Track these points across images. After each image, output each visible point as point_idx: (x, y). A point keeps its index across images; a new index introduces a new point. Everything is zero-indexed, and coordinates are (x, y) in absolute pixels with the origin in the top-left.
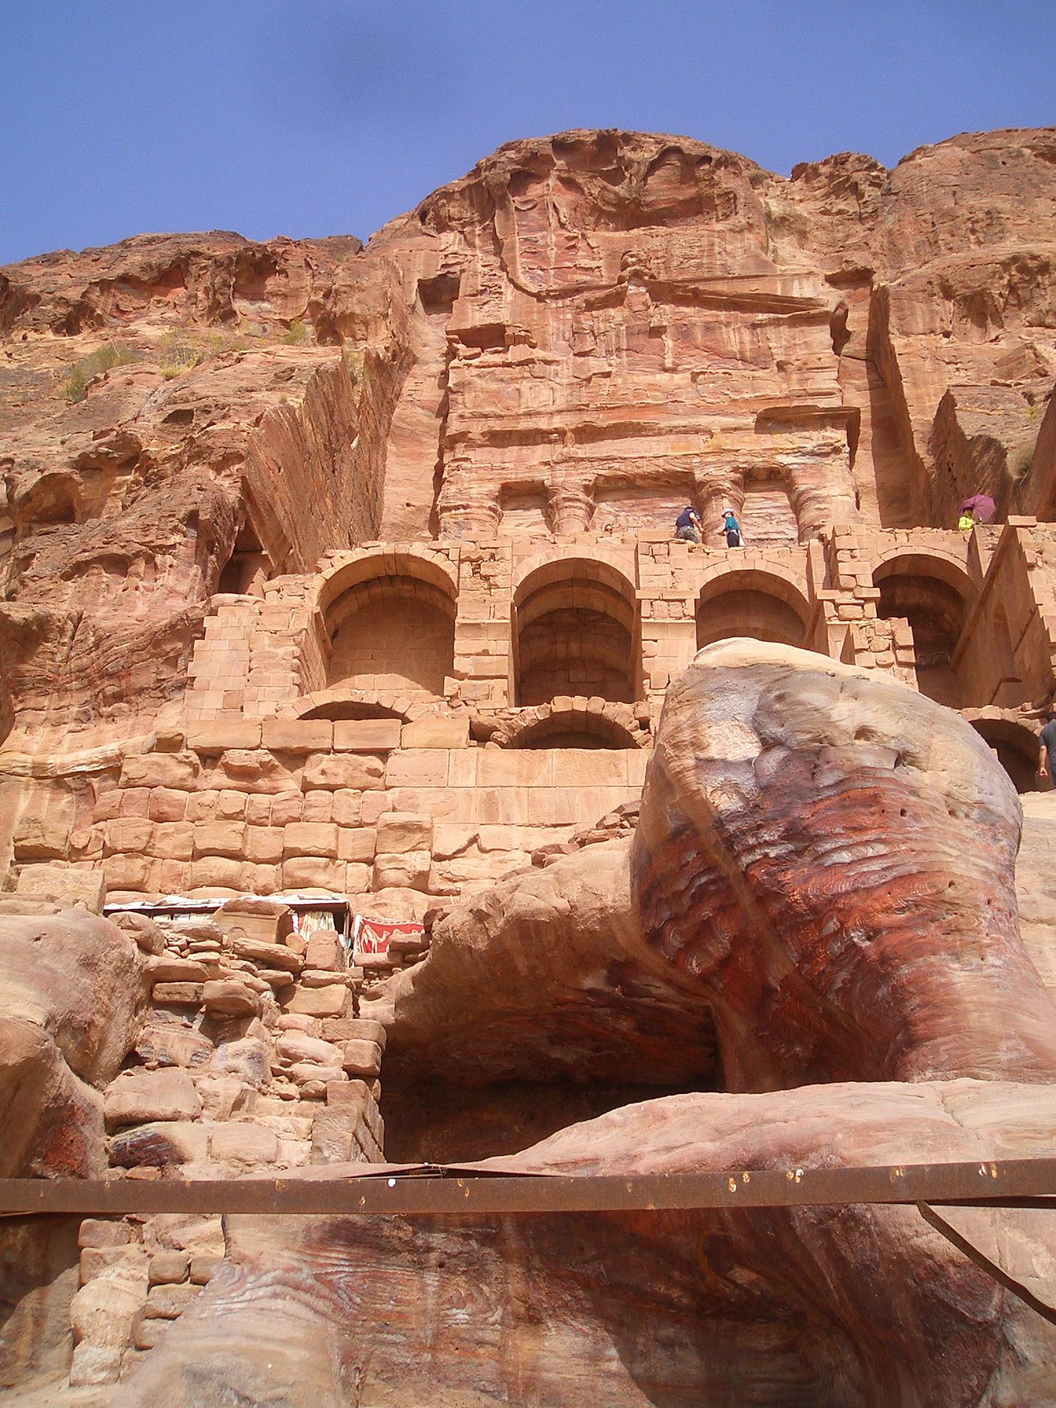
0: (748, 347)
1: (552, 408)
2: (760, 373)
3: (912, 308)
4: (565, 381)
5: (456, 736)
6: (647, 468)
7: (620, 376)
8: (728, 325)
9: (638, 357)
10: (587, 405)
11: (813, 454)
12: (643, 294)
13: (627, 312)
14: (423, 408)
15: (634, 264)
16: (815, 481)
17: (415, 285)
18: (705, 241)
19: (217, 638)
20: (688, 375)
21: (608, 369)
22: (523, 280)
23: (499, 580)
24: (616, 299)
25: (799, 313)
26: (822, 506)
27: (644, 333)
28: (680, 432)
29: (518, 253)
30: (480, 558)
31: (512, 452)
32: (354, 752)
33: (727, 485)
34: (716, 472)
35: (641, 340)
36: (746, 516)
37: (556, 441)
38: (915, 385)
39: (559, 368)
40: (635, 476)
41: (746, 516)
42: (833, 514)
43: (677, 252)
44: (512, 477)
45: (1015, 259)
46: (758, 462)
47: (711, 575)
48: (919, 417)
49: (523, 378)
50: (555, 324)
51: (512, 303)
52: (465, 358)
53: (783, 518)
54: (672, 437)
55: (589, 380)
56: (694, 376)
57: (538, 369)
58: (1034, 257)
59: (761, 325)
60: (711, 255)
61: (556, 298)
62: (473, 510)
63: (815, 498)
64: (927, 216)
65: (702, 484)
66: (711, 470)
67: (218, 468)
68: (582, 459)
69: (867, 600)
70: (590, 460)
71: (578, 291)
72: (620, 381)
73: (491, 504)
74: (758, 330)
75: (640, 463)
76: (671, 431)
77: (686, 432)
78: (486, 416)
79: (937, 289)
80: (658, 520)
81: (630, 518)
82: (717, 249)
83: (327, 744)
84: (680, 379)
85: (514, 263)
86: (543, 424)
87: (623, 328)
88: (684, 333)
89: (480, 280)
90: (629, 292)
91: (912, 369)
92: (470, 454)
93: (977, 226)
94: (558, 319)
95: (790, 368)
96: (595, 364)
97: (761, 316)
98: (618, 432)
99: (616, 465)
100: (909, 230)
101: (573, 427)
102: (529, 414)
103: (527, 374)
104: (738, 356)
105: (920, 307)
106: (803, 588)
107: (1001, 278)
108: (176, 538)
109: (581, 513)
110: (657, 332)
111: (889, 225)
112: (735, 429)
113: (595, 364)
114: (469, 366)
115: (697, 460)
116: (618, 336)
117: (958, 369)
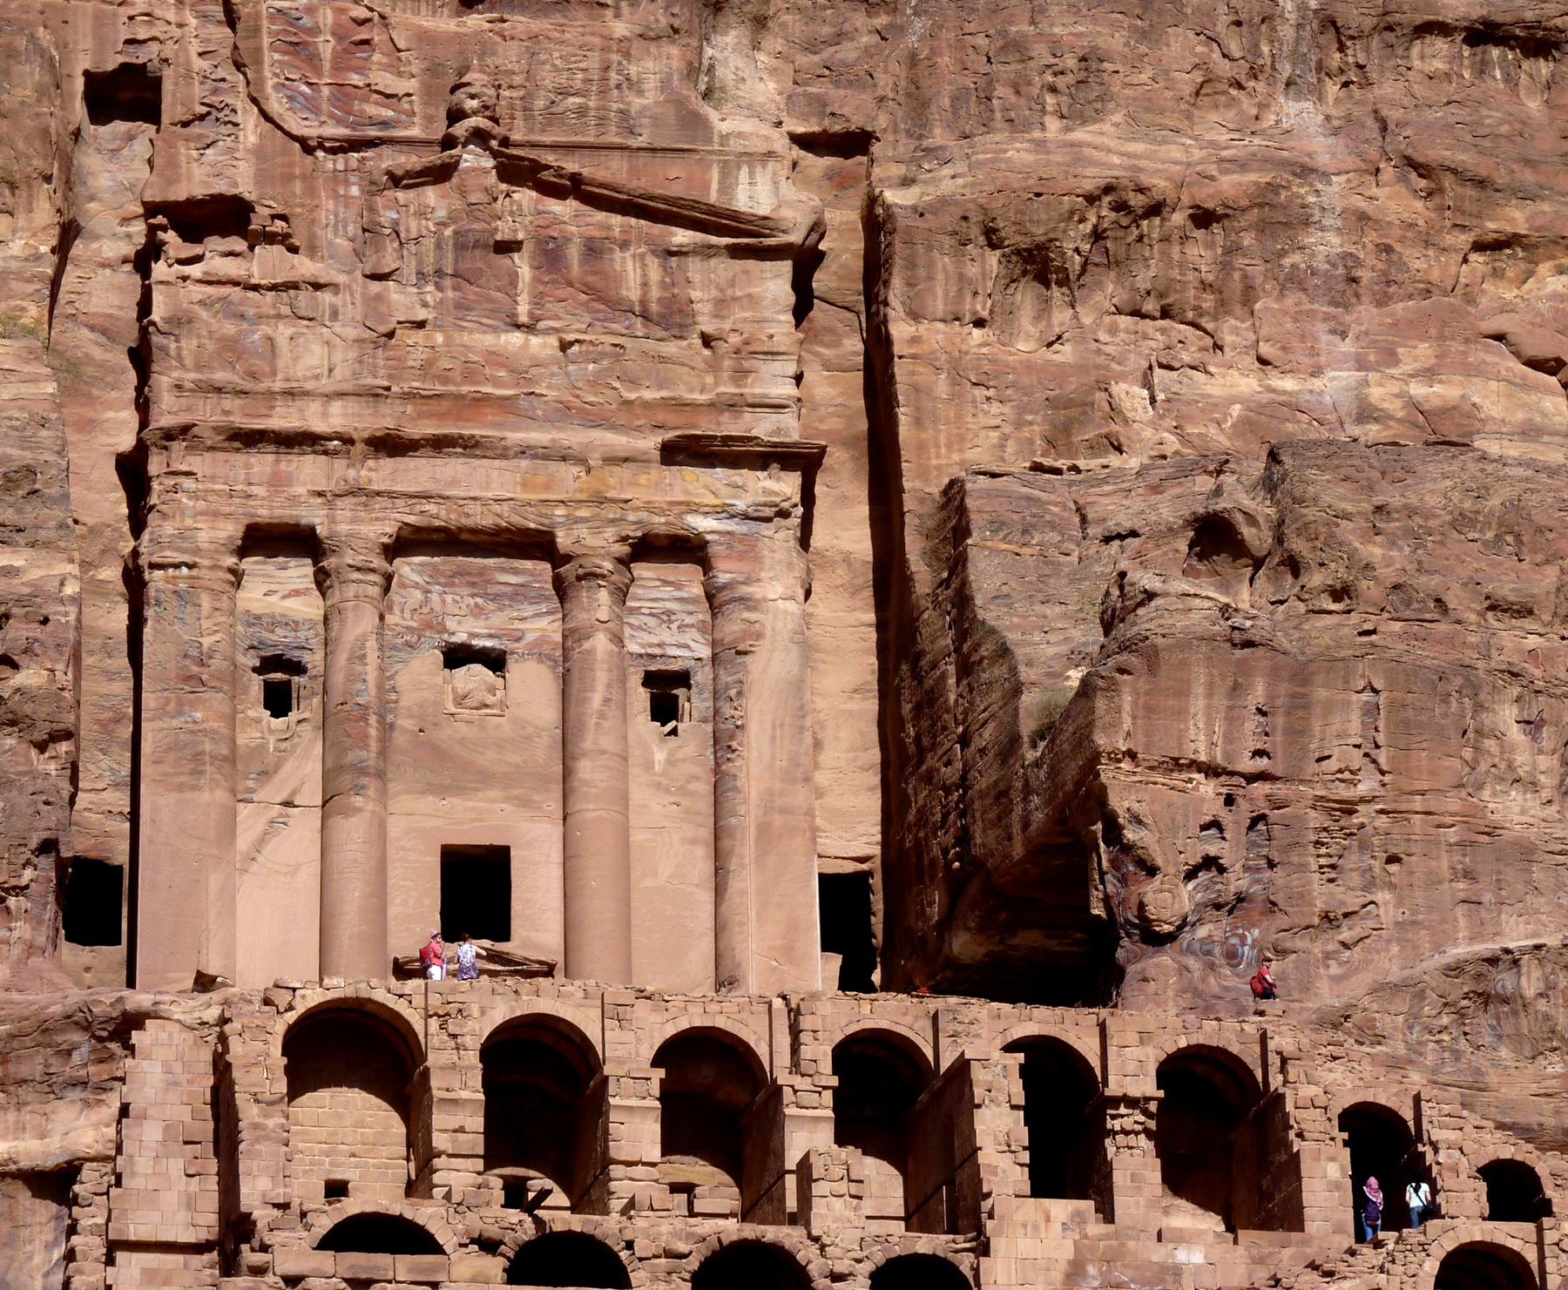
0: (655, 293)
1: (326, 384)
2: (671, 348)
3: (931, 265)
4: (351, 333)
5: (493, 1272)
6: (482, 518)
7: (439, 327)
8: (624, 245)
9: (471, 292)
10: (388, 389)
11: (746, 517)
12: (486, 171)
13: (458, 204)
14: (92, 328)
15: (475, 113)
16: (744, 567)
17: (79, 84)
18: (593, 62)
19: (148, 1057)
20: (553, 341)
21: (421, 314)
22: (276, 105)
23: (468, 1040)
24: (440, 174)
25: (747, 239)
26: (753, 616)
27: (486, 246)
28: (535, 457)
29: (266, 41)
30: (448, 1014)
31: (261, 462)
32: (413, 1283)
33: (608, 565)
34: (592, 540)
35: (477, 261)
36: (632, 611)
37: (336, 453)
38: (918, 422)
39: (338, 300)
40: (461, 529)
41: (632, 611)
42: (768, 632)
43: (548, 79)
44: (265, 513)
45: (1108, 189)
46: (659, 524)
47: (670, 1031)
48: (918, 484)
49: (279, 316)
50: (331, 205)
51: (259, 153)
52: (181, 262)
53: (689, 620)
54: (524, 463)
55: (390, 335)
56: (564, 346)
57: (303, 297)
58: (1141, 190)
59: (680, 253)
60: (603, 92)
61: (332, 151)
62: (204, 573)
63: (742, 599)
64: (981, 41)
65: (568, 558)
66: (583, 531)
67: (41, 747)
68: (378, 494)
69: (825, 1088)
70: (391, 495)
71: (371, 143)
72: (439, 338)
73: (231, 561)
74: (674, 261)
75: (472, 508)
76: (523, 451)
77: (546, 458)
78: (219, 390)
79: (975, 232)
80: (491, 606)
81: (449, 598)
82: (614, 77)
83: (390, 1276)
84: (541, 345)
85: (259, 62)
86: (315, 418)
87: (448, 232)
88: (550, 255)
89: (198, 91)
90: (463, 165)
91: (916, 389)
92: (195, 463)
93: (1061, 82)
94: (336, 196)
95: (722, 347)
96: (401, 300)
97: (682, 237)
98: (440, 444)
99: (431, 508)
100: (945, 60)
101: (366, 435)
102: (290, 394)
103: (286, 310)
104: (637, 309)
105: (944, 262)
106: (762, 1051)
107: (1081, 221)
108: (28, 874)
109: (375, 591)
110: (507, 247)
111: (912, 40)
112: (626, 460)
113: (401, 300)
114: (185, 278)
115: (560, 511)
116: (438, 246)
117: (988, 399)
